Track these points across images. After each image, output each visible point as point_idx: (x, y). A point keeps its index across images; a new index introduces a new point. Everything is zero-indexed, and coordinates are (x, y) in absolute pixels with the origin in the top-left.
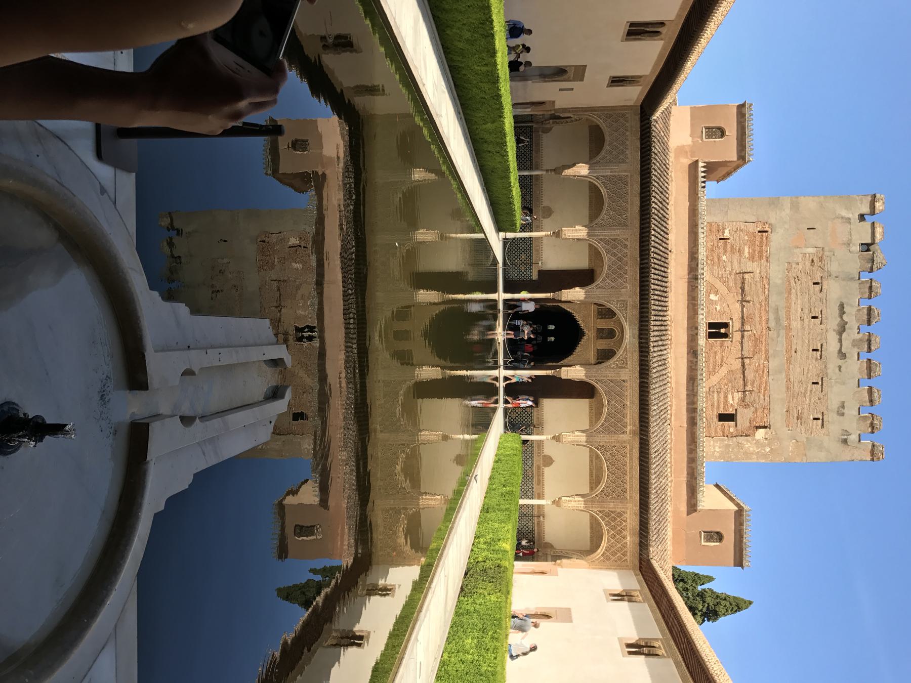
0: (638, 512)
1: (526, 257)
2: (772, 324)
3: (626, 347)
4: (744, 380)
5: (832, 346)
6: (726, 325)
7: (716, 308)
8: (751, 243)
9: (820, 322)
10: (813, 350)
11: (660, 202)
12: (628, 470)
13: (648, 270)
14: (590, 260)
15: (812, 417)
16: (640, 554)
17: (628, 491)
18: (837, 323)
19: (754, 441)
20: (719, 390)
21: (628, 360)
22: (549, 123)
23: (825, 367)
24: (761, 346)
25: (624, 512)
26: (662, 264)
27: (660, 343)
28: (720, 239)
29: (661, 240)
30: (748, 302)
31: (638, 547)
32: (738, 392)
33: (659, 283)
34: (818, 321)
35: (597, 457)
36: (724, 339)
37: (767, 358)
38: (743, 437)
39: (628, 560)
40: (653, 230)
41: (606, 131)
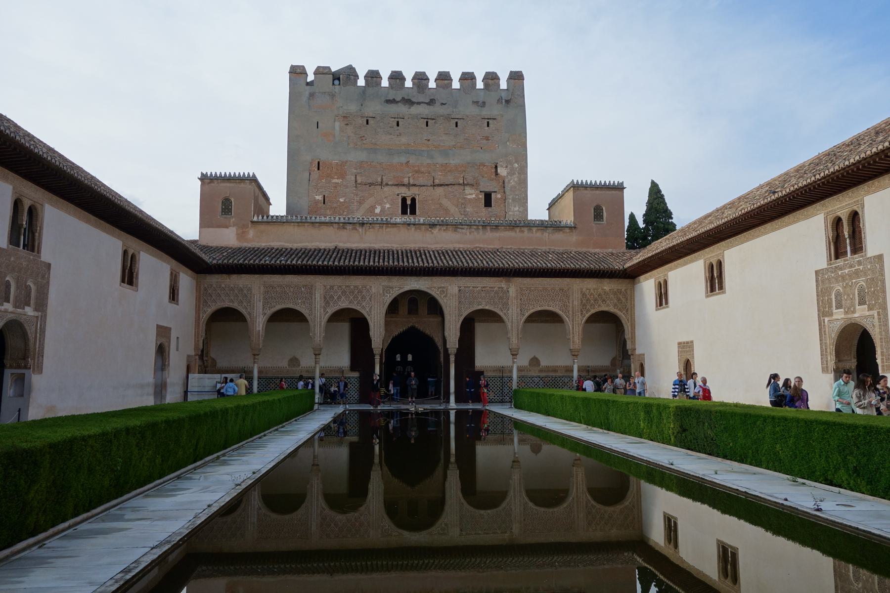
0: (581, 280)
2: (403, 160)
4: (454, 184)
5: (423, 110)
6: (404, 200)
7: (388, 208)
9: (402, 119)
10: (427, 125)
11: (291, 256)
15: (487, 128)
16: (620, 278)
18: (402, 105)
20: (463, 206)
21: (440, 286)
23: (441, 116)
25: (582, 292)
26: (349, 255)
27: (424, 257)
28: (324, 203)
29: (327, 255)
31: (613, 279)
33: (367, 258)
34: (400, 120)
35: (530, 316)
36: (417, 202)
40: (317, 263)
41: (220, 305)
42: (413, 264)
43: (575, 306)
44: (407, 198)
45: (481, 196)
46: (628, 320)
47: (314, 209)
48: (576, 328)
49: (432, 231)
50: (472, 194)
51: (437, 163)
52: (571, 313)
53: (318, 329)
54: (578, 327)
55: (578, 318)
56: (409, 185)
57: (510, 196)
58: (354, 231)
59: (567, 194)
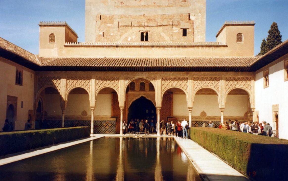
0: (226, 72)
1: (105, 123)
2: (142, 13)
3: (147, 77)
4: (167, 25)
6: (142, 34)
7: (134, 38)
8: (105, 22)
12: (205, 77)
13: (123, 68)
14: (107, 94)
16: (247, 71)
17: (216, 77)
19: (196, 20)
22: (42, 112)
24: (151, 18)
28: (103, 36)
30: (132, 23)
31: (244, 72)
32: (172, 28)
37: (158, 15)
38: (194, 25)
39: (251, 77)
43: (222, 86)
45: (181, 31)
46: (251, 93)
47: (98, 38)
50: (176, 30)
51: (159, 15)
52: (220, 89)
56: (145, 26)
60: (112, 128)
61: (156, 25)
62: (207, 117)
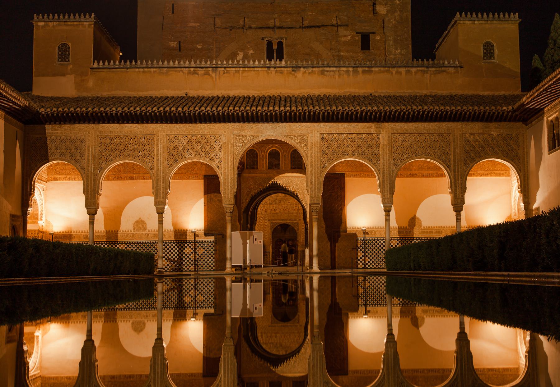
4: (326, 26)
6: (269, 44)
36: (284, 46)
42: (267, 108)
43: (458, 153)
44: (273, 42)
45: (357, 38)
48: (458, 180)
49: (296, 75)
52: (452, 162)
53: (162, 185)
54: (461, 178)
55: (461, 169)
56: (274, 28)
57: (391, 37)
58: (206, 76)
59: (452, 30)
60: (206, 258)
61: (302, 26)
62: (424, 227)
